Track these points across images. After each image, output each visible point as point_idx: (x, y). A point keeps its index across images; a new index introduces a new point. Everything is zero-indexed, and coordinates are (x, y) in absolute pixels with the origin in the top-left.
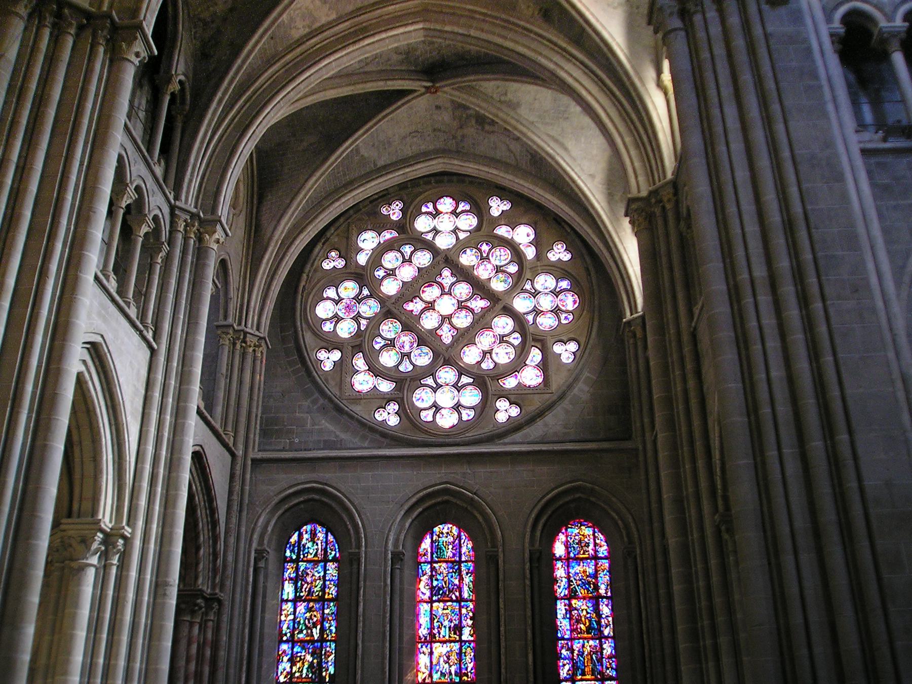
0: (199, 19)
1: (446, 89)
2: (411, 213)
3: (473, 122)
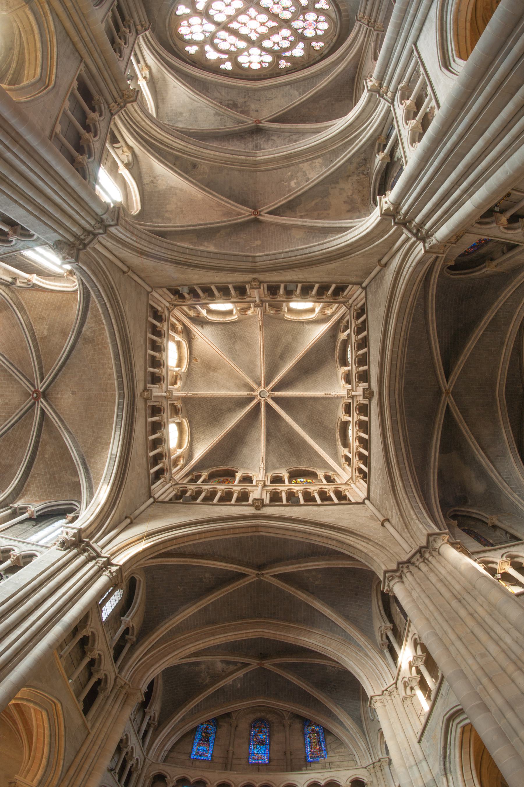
0: (365, 175)
1: (251, 122)
2: (275, 64)
3: (239, 105)
